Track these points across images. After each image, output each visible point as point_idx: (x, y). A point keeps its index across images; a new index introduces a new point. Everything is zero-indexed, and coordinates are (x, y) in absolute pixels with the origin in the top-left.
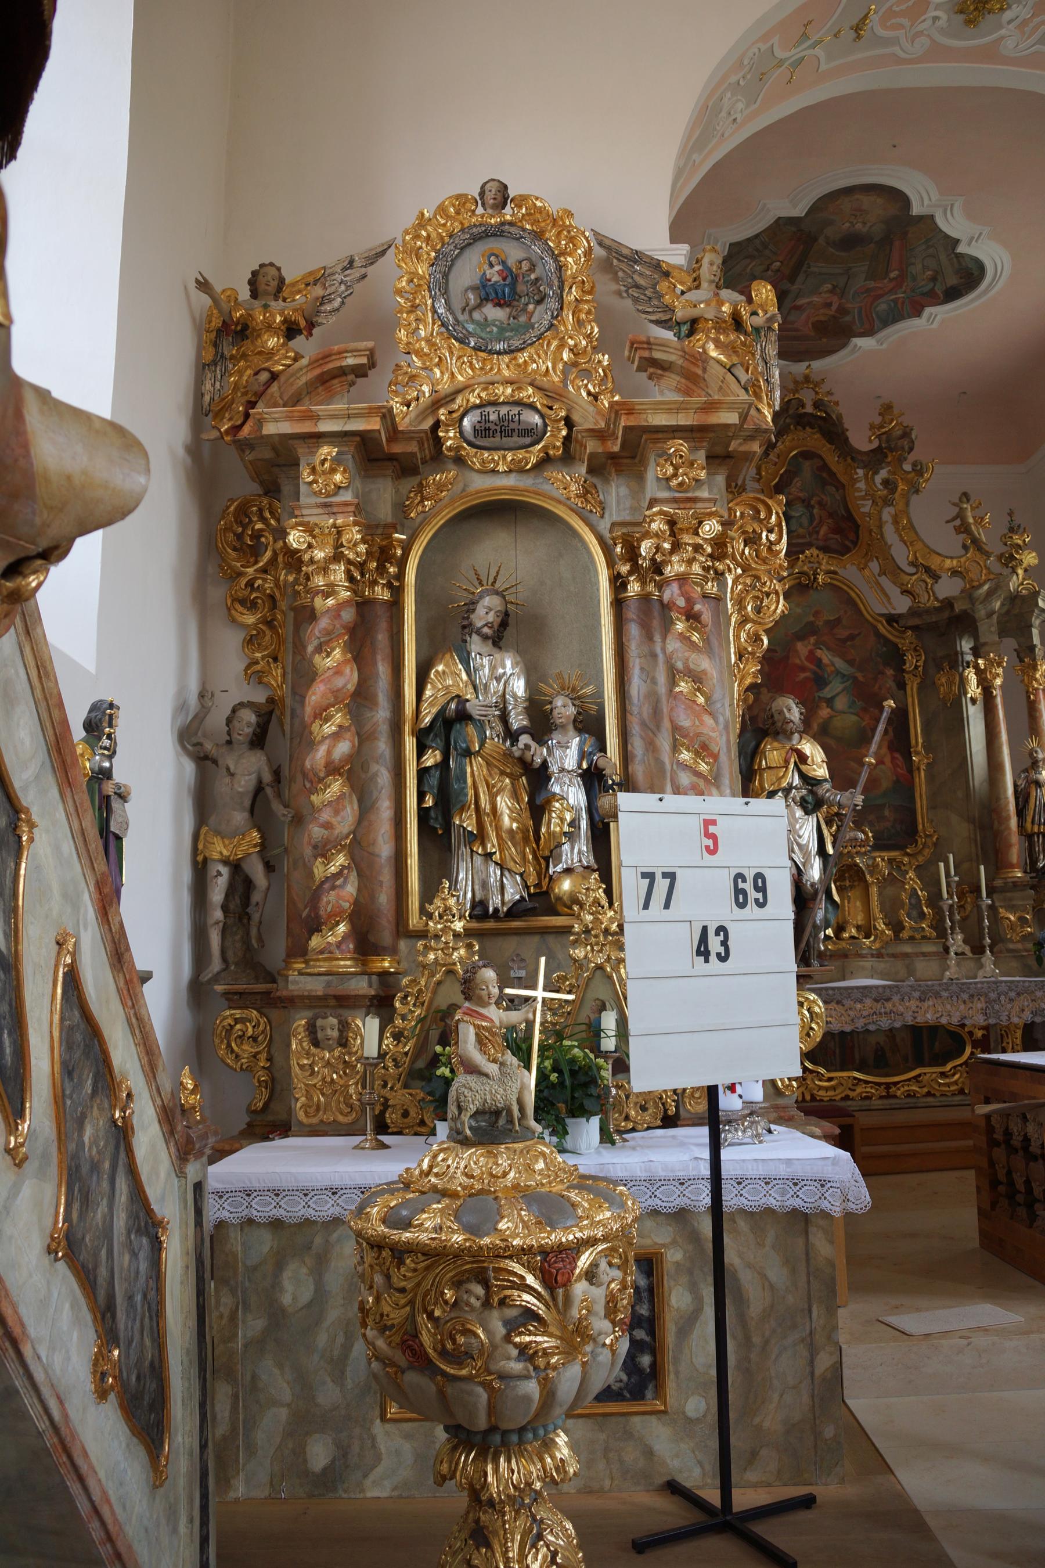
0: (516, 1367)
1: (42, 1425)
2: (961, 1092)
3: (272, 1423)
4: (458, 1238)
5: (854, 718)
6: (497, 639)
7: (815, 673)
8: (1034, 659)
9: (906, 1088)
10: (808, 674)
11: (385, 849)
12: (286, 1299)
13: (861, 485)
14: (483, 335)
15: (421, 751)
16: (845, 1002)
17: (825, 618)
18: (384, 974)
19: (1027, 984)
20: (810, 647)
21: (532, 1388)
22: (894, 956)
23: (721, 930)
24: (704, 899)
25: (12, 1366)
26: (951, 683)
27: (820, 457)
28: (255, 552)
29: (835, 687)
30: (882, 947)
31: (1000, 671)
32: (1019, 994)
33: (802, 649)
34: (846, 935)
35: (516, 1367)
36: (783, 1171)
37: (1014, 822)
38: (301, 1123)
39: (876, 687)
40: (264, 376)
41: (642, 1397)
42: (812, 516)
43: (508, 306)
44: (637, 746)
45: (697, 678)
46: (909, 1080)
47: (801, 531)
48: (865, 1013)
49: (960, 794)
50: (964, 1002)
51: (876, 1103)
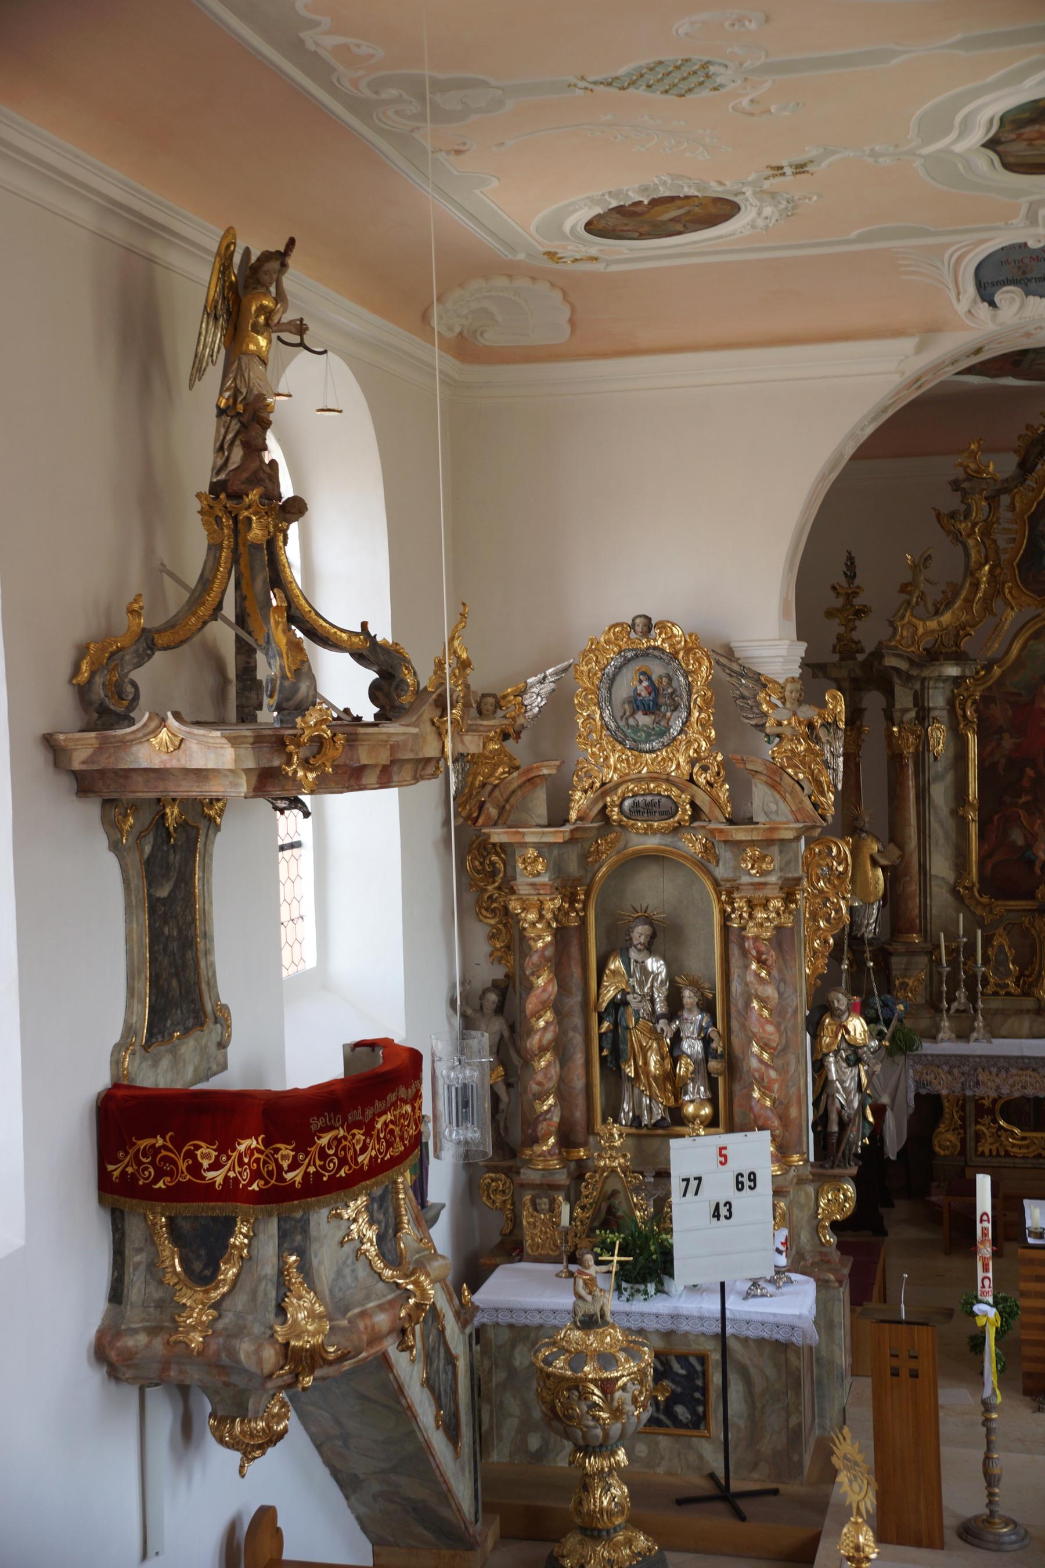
0: (591, 1423)
1: (422, 1440)
3: (511, 1425)
4: (569, 1373)
6: (650, 948)
11: (579, 1083)
12: (517, 1363)
14: (635, 738)
15: (600, 1022)
16: (1040, 1070)
18: (580, 1162)
21: (599, 1432)
23: (728, 1204)
24: (719, 1186)
25: (414, 1424)
28: (493, 874)
35: (591, 1423)
36: (771, 1319)
38: (528, 1255)
40: (489, 788)
41: (699, 1428)
43: (653, 713)
44: (735, 1025)
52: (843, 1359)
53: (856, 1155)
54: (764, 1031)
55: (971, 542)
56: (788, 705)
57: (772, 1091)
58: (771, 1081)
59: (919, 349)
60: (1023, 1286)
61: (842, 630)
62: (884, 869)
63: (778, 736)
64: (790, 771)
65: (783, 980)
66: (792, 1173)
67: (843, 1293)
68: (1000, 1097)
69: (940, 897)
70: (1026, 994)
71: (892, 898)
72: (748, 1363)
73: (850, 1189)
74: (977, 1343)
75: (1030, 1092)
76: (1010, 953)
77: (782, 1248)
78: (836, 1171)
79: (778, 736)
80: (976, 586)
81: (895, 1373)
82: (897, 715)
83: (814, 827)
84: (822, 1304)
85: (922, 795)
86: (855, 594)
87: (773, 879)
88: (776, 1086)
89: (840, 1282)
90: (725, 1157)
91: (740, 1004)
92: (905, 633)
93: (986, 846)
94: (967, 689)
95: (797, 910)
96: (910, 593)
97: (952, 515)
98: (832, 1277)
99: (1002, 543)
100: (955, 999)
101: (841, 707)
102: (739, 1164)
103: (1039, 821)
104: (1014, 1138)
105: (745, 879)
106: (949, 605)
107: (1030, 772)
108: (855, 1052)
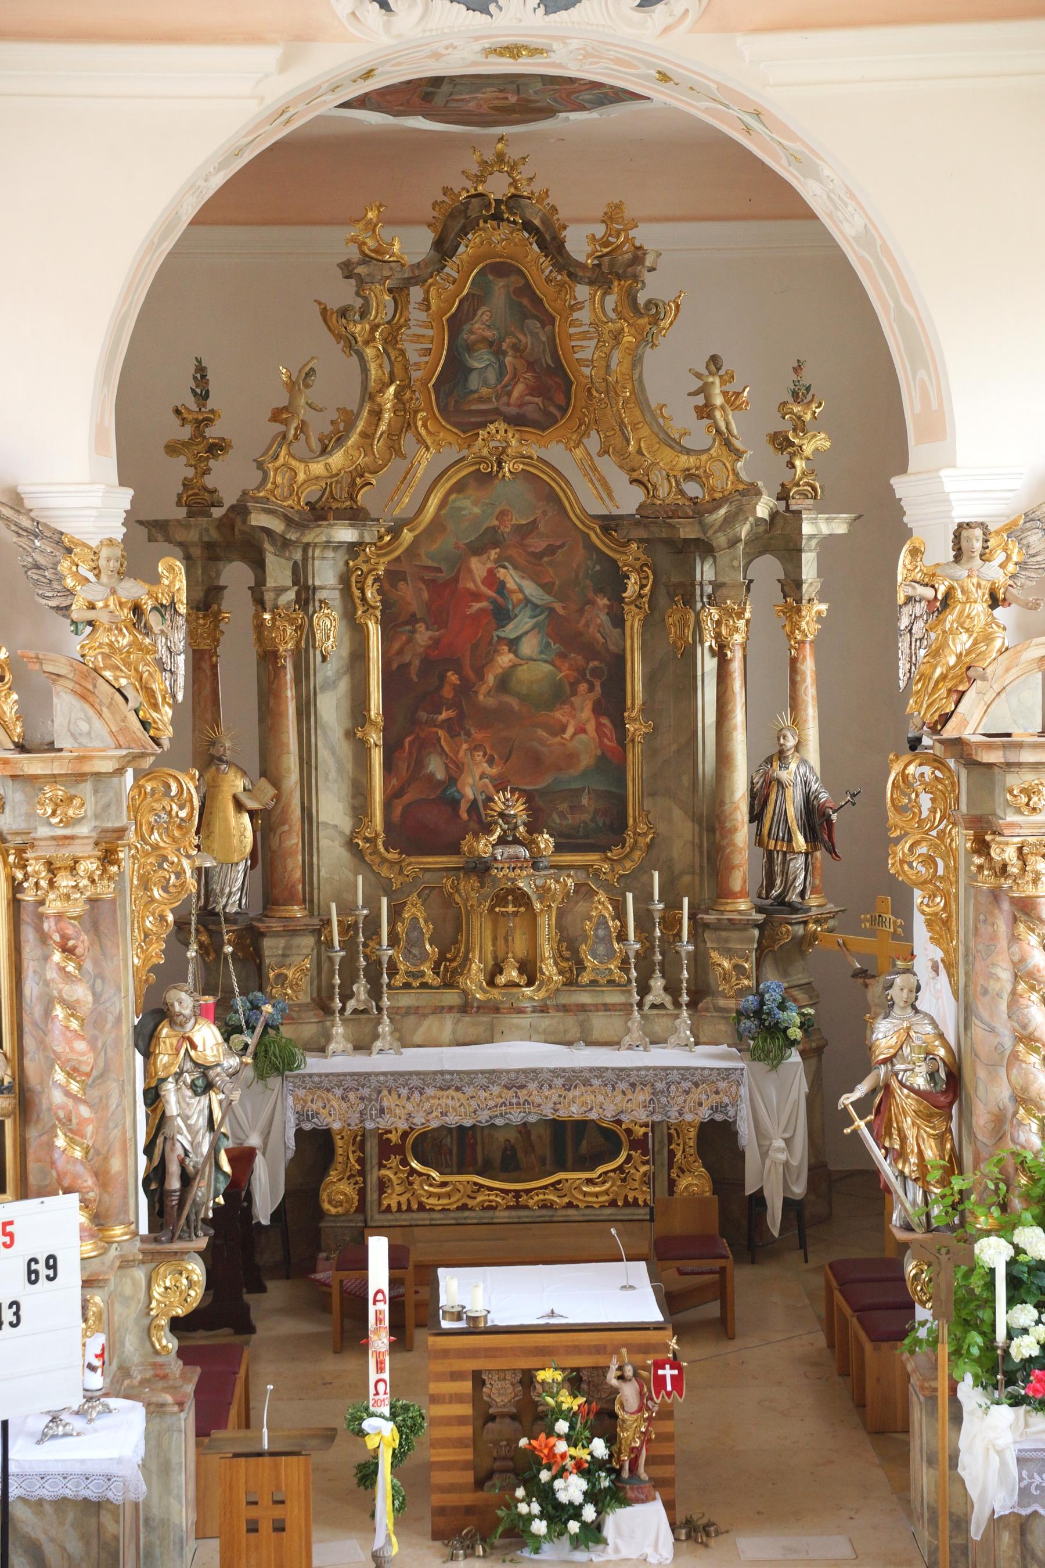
2: (613, 1203)
5: (547, 668)
7: (494, 602)
8: (799, 601)
9: (541, 1197)
10: (484, 604)
13: (584, 316)
16: (465, 1089)
17: (514, 522)
19: (706, 1072)
20: (489, 565)
22: (565, 1008)
23: (15, 1304)
26: (683, 623)
27: (521, 273)
29: (522, 623)
30: (549, 998)
31: (741, 624)
32: (696, 1085)
33: (478, 567)
34: (501, 980)
36: (78, 1469)
37: (743, 834)
39: (583, 621)
42: (502, 366)
44: (29, 1042)
45: (71, 1007)
46: (545, 1187)
47: (484, 391)
48: (491, 1103)
49: (686, 780)
50: (624, 1093)
51: (501, 1215)
52: (182, 1514)
53: (205, 1221)
54: (72, 1049)
55: (369, 352)
56: (104, 578)
57: (83, 1136)
58: (83, 1122)
59: (285, 65)
60: (435, 1388)
61: (190, 473)
62: (252, 814)
63: (90, 623)
64: (108, 674)
65: (100, 975)
66: (113, 1252)
67: (186, 1420)
68: (412, 1129)
69: (332, 853)
70: (448, 985)
71: (265, 856)
72: (42, 1537)
73: (197, 1270)
74: (367, 1474)
75: (452, 1120)
76: (427, 930)
77: (97, 1363)
78: (177, 1246)
79: (90, 623)
80: (377, 414)
81: (253, 1528)
82: (269, 597)
83: (143, 755)
84: (154, 1440)
85: (306, 710)
86: (208, 421)
87: (83, 830)
88: (89, 1129)
89: (181, 1404)
90: (11, 1235)
91: (38, 1012)
92: (279, 480)
93: (394, 782)
94: (367, 561)
95: (121, 874)
96: (286, 422)
97: (343, 313)
98: (169, 1398)
99: (413, 357)
100: (352, 995)
101: (181, 583)
102: (32, 1244)
103: (465, 746)
104: (431, 1185)
105: (43, 831)
106: (340, 440)
107: (453, 677)
108: (205, 1075)
